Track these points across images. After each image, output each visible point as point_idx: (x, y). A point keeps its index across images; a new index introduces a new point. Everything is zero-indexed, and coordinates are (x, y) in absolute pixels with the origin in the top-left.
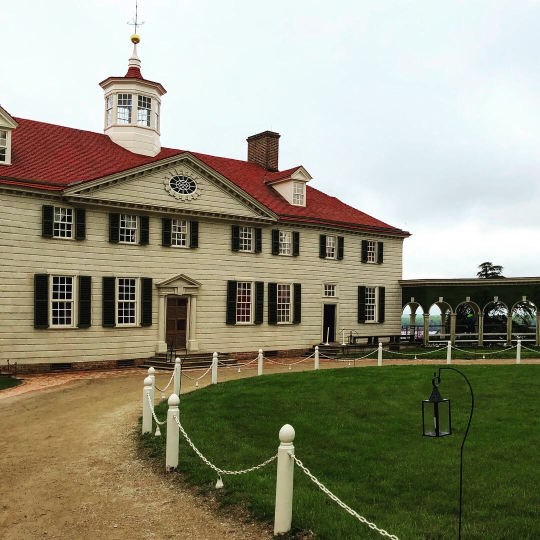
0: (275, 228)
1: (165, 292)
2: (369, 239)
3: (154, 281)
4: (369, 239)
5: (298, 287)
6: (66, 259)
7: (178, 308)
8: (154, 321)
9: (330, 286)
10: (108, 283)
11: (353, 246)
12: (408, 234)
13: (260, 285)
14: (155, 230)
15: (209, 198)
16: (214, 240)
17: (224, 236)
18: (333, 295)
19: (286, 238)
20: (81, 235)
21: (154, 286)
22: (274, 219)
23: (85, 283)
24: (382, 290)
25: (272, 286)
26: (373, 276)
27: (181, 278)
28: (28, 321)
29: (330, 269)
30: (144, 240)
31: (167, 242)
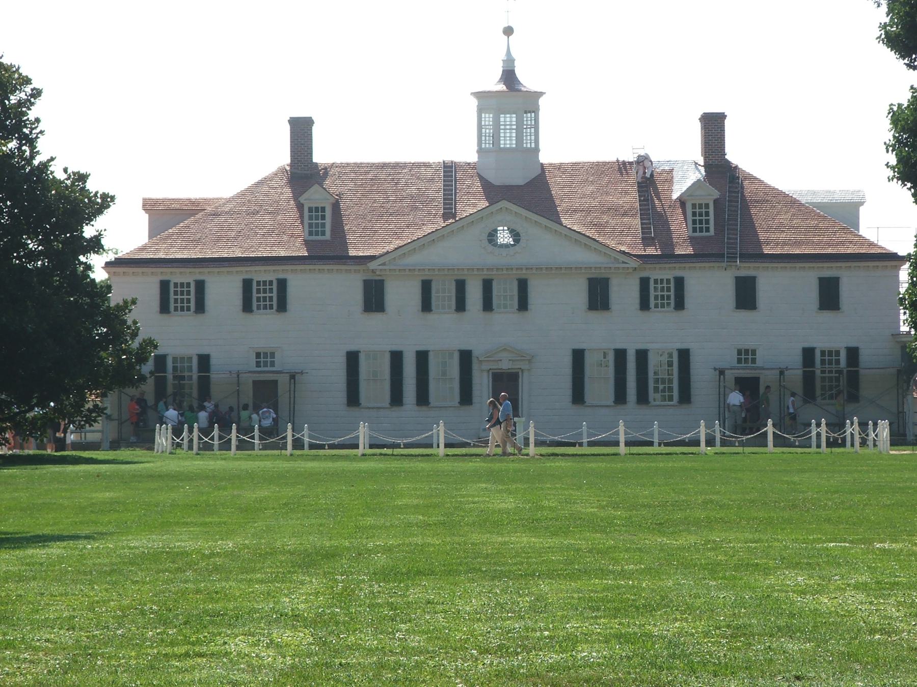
0: (645, 274)
1: (485, 366)
3: (475, 354)
6: (377, 336)
7: (507, 383)
8: (475, 399)
9: (747, 351)
10: (422, 357)
13: (620, 355)
14: (474, 294)
18: (754, 361)
21: (474, 361)
23: (397, 358)
25: (642, 356)
31: (488, 305)
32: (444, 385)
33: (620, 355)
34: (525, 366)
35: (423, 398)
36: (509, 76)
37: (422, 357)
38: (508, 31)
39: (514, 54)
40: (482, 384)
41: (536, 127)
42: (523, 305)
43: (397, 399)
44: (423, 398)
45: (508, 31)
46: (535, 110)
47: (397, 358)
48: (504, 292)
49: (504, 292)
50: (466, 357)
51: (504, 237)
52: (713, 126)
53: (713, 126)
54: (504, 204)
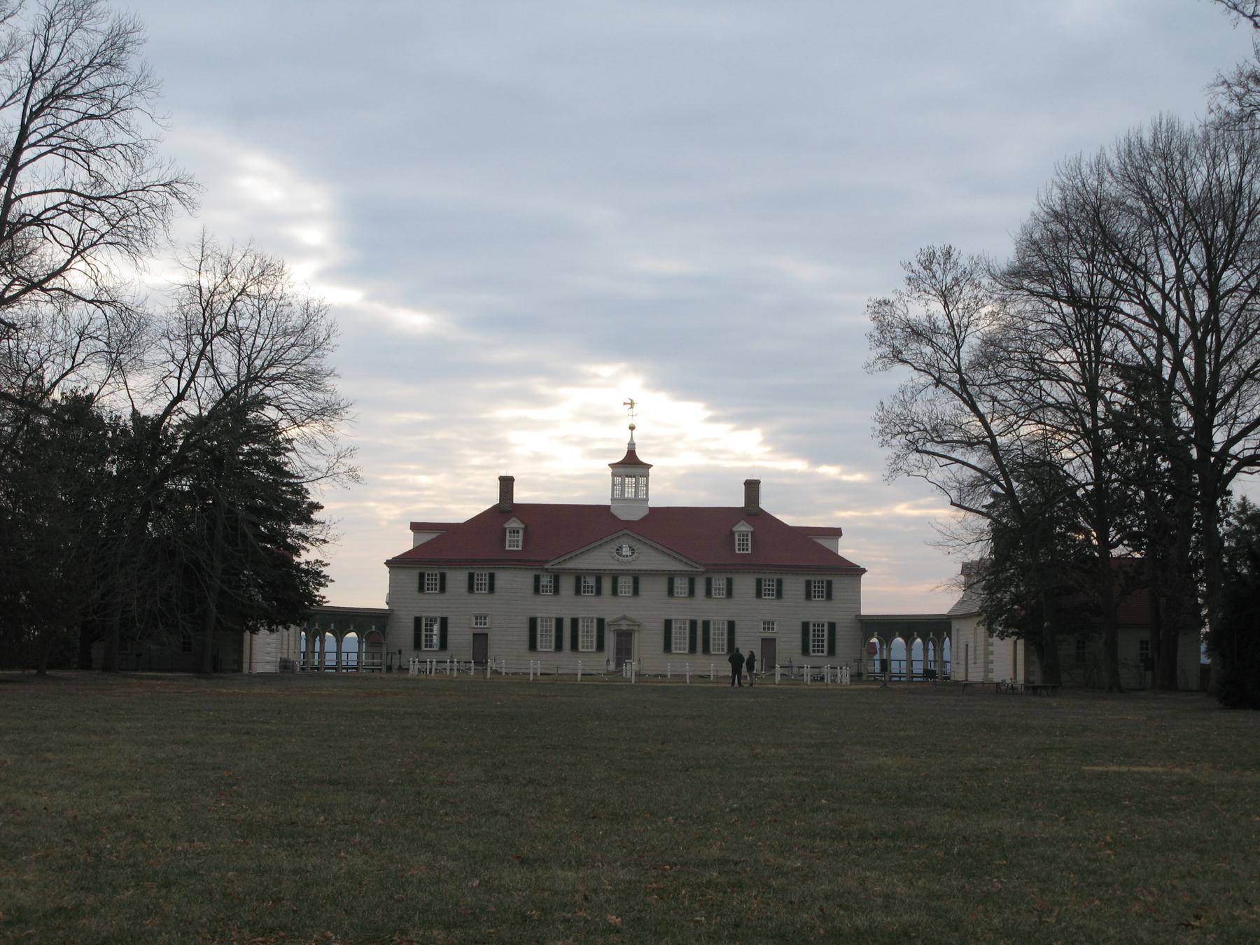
2: (812, 578)
3: (607, 620)
4: (812, 578)
5: (731, 625)
6: (549, 608)
8: (606, 647)
10: (575, 622)
11: (794, 586)
12: (864, 571)
14: (607, 584)
15: (650, 559)
16: (653, 590)
17: (662, 585)
19: (719, 583)
20: (556, 591)
22: (701, 569)
23: (559, 622)
24: (832, 626)
26: (819, 612)
27: (624, 618)
28: (526, 645)
29: (768, 607)
30: (599, 592)
31: (615, 592)
32: (587, 639)
33: (693, 624)
34: (636, 628)
35: (574, 646)
36: (631, 454)
37: (575, 622)
38: (632, 428)
39: (635, 441)
40: (610, 640)
41: (647, 485)
42: (636, 592)
43: (559, 647)
44: (574, 646)
45: (632, 428)
46: (647, 476)
47: (559, 622)
48: (625, 584)
49: (625, 584)
50: (601, 622)
51: (626, 551)
52: (752, 487)
53: (752, 487)
54: (626, 531)
